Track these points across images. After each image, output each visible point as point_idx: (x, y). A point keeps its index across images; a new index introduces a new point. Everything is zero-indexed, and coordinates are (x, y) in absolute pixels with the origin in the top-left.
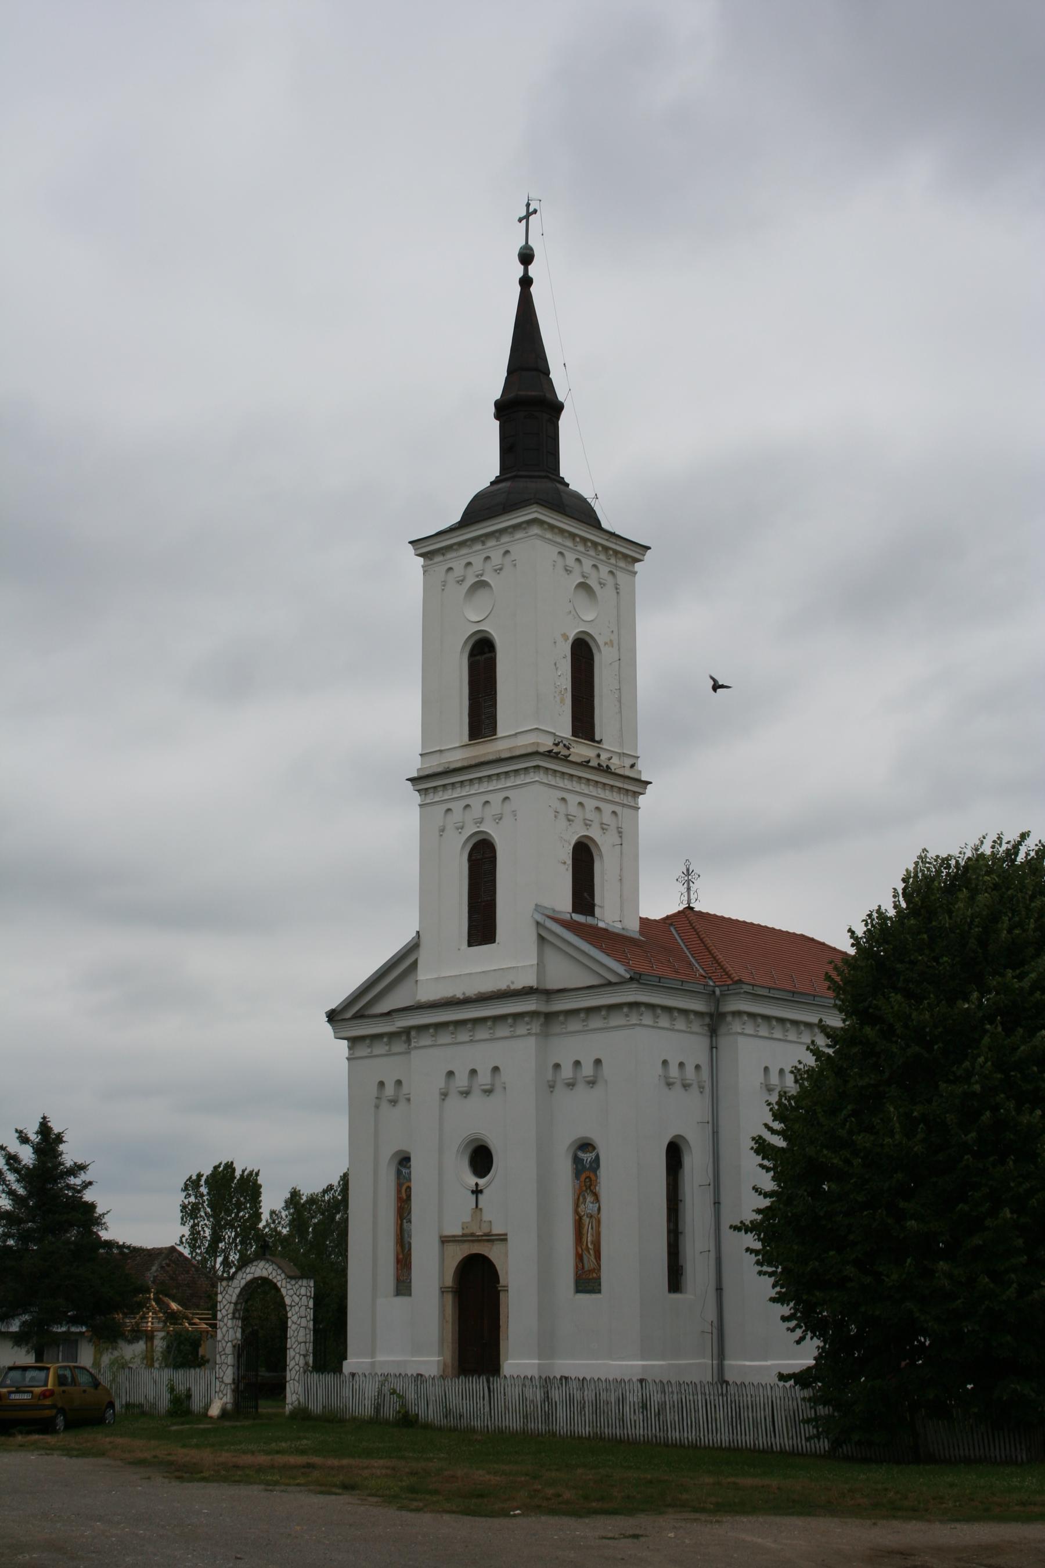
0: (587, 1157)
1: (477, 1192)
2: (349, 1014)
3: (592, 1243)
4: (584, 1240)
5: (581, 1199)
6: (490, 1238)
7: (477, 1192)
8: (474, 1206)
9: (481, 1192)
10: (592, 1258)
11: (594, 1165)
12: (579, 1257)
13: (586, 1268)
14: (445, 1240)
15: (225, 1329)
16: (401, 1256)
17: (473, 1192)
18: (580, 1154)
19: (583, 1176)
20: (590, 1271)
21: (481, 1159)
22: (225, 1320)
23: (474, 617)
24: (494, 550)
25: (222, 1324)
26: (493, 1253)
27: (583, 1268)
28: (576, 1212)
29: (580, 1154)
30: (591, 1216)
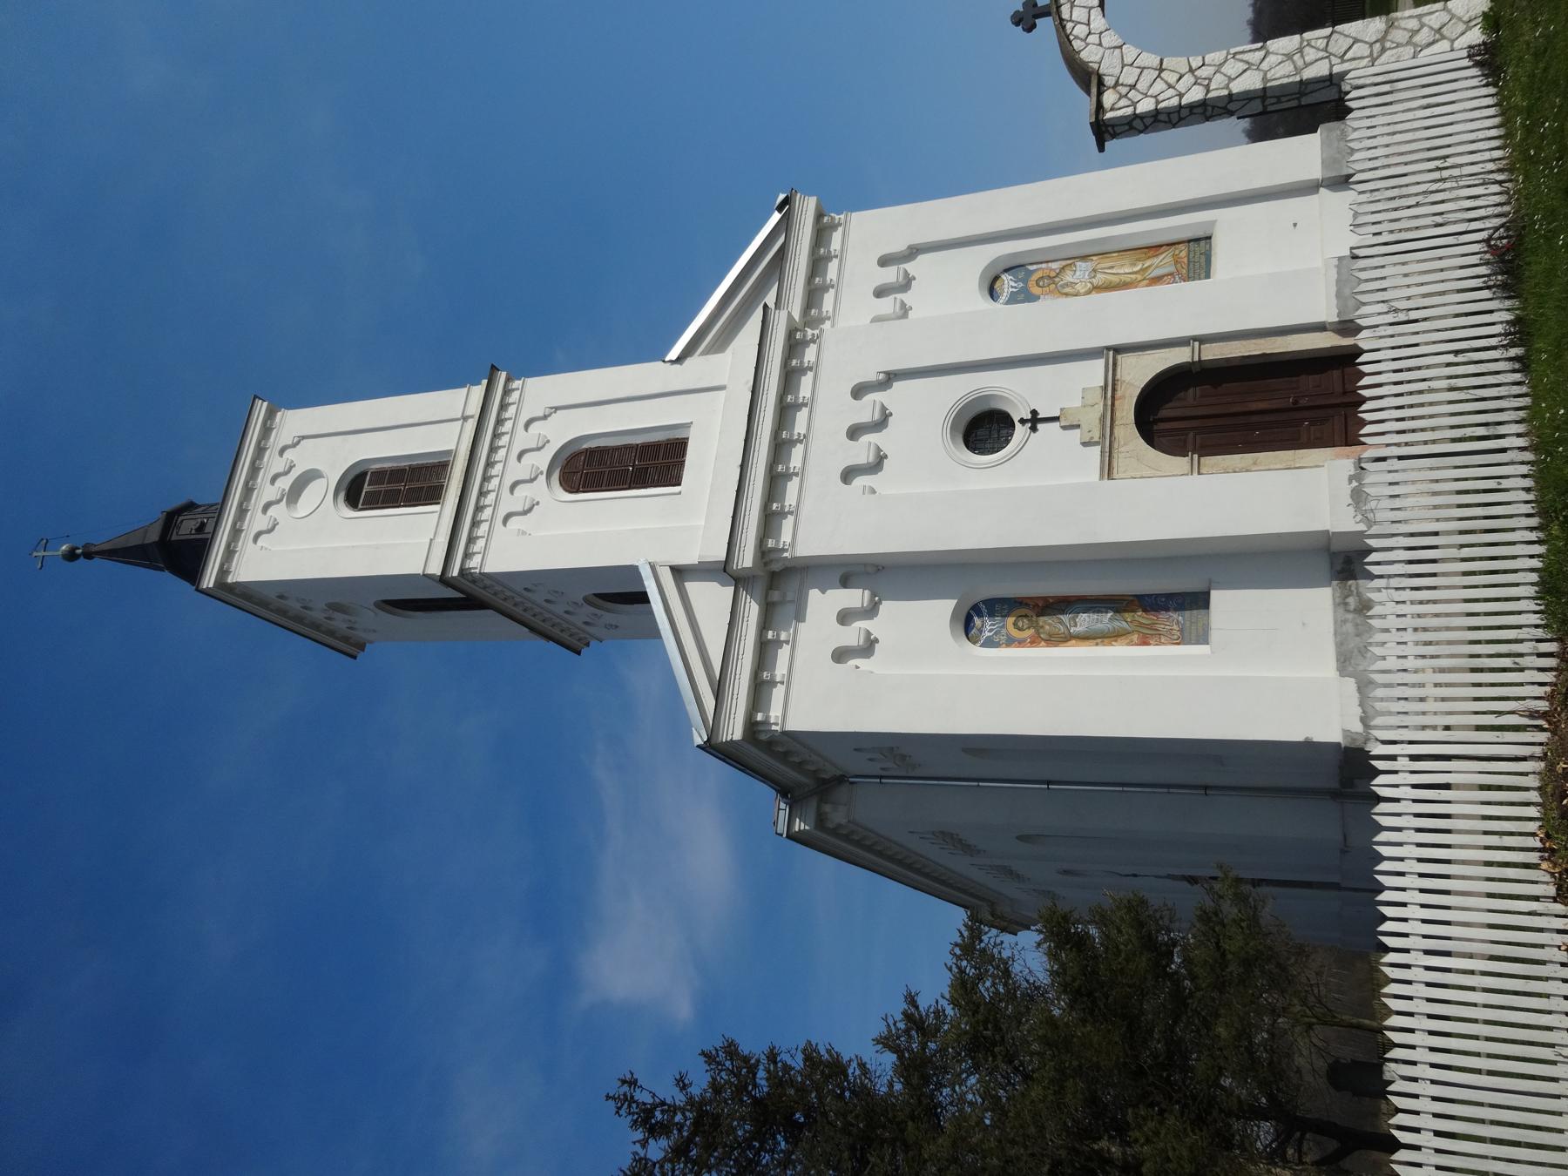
0: (1008, 283)
1: (1034, 421)
2: (709, 702)
3: (1134, 265)
4: (1127, 278)
5: (1067, 290)
6: (1111, 387)
7: (1034, 421)
8: (1056, 425)
9: (1034, 413)
10: (1156, 261)
11: (1021, 275)
12: (1157, 280)
13: (1172, 269)
14: (1108, 470)
15: (1232, 68)
16: (1135, 637)
17: (1034, 429)
18: (1004, 298)
19: (1035, 290)
20: (1176, 262)
21: (985, 429)
22: (1204, 72)
23: (319, 494)
24: (273, 463)
25: (1218, 81)
26: (1138, 373)
27: (1171, 274)
28: (1089, 292)
29: (1004, 298)
30: (1094, 271)
